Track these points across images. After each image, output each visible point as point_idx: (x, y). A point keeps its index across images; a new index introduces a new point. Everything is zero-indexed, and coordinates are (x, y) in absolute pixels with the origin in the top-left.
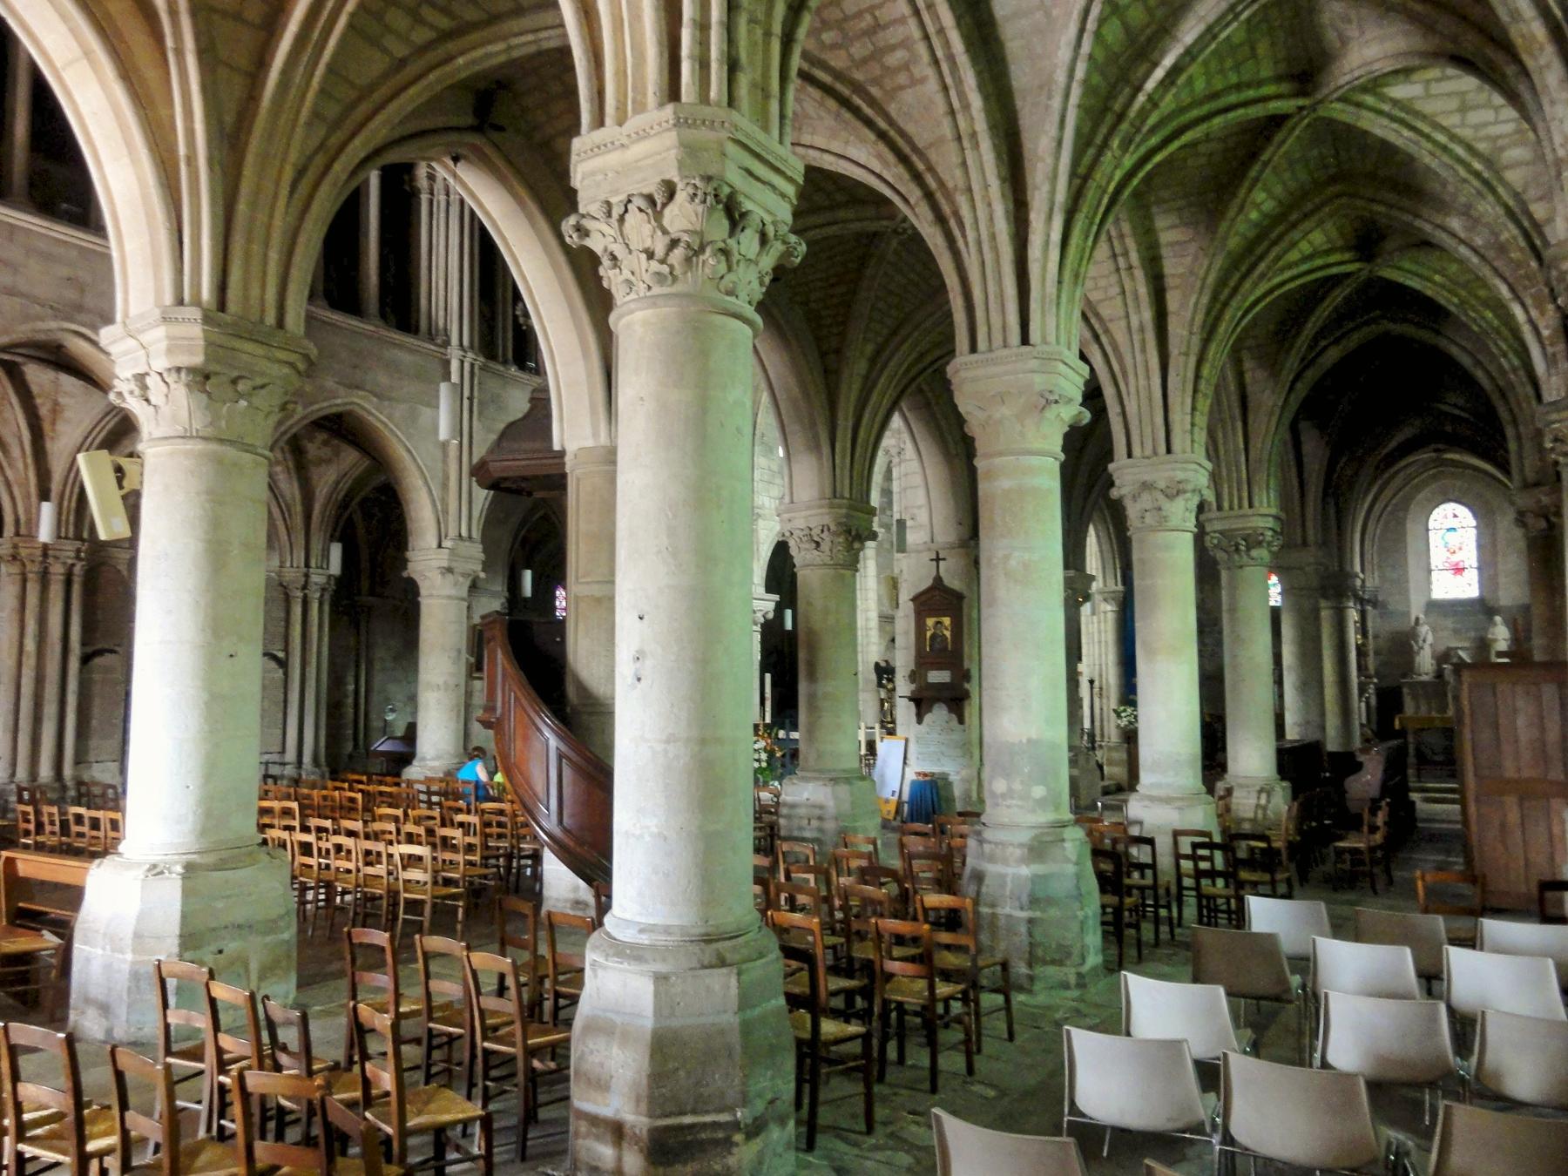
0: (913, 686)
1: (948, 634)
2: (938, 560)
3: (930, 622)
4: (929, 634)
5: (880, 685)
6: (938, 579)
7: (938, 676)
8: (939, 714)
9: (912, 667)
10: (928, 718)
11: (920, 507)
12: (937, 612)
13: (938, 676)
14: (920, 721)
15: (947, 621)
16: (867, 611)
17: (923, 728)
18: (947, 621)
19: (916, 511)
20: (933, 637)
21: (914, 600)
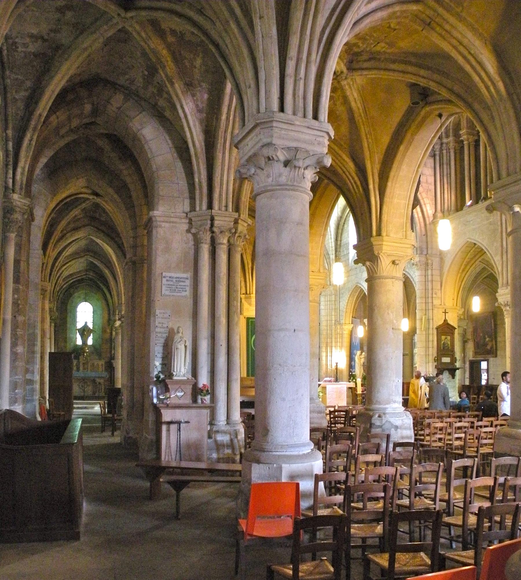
0: (436, 364)
1: (449, 343)
2: (445, 313)
3: (443, 337)
4: (442, 342)
6: (445, 320)
7: (446, 360)
9: (435, 355)
11: (438, 290)
12: (445, 334)
13: (446, 360)
15: (449, 338)
18: (449, 338)
19: (437, 291)
20: (444, 344)
21: (437, 329)
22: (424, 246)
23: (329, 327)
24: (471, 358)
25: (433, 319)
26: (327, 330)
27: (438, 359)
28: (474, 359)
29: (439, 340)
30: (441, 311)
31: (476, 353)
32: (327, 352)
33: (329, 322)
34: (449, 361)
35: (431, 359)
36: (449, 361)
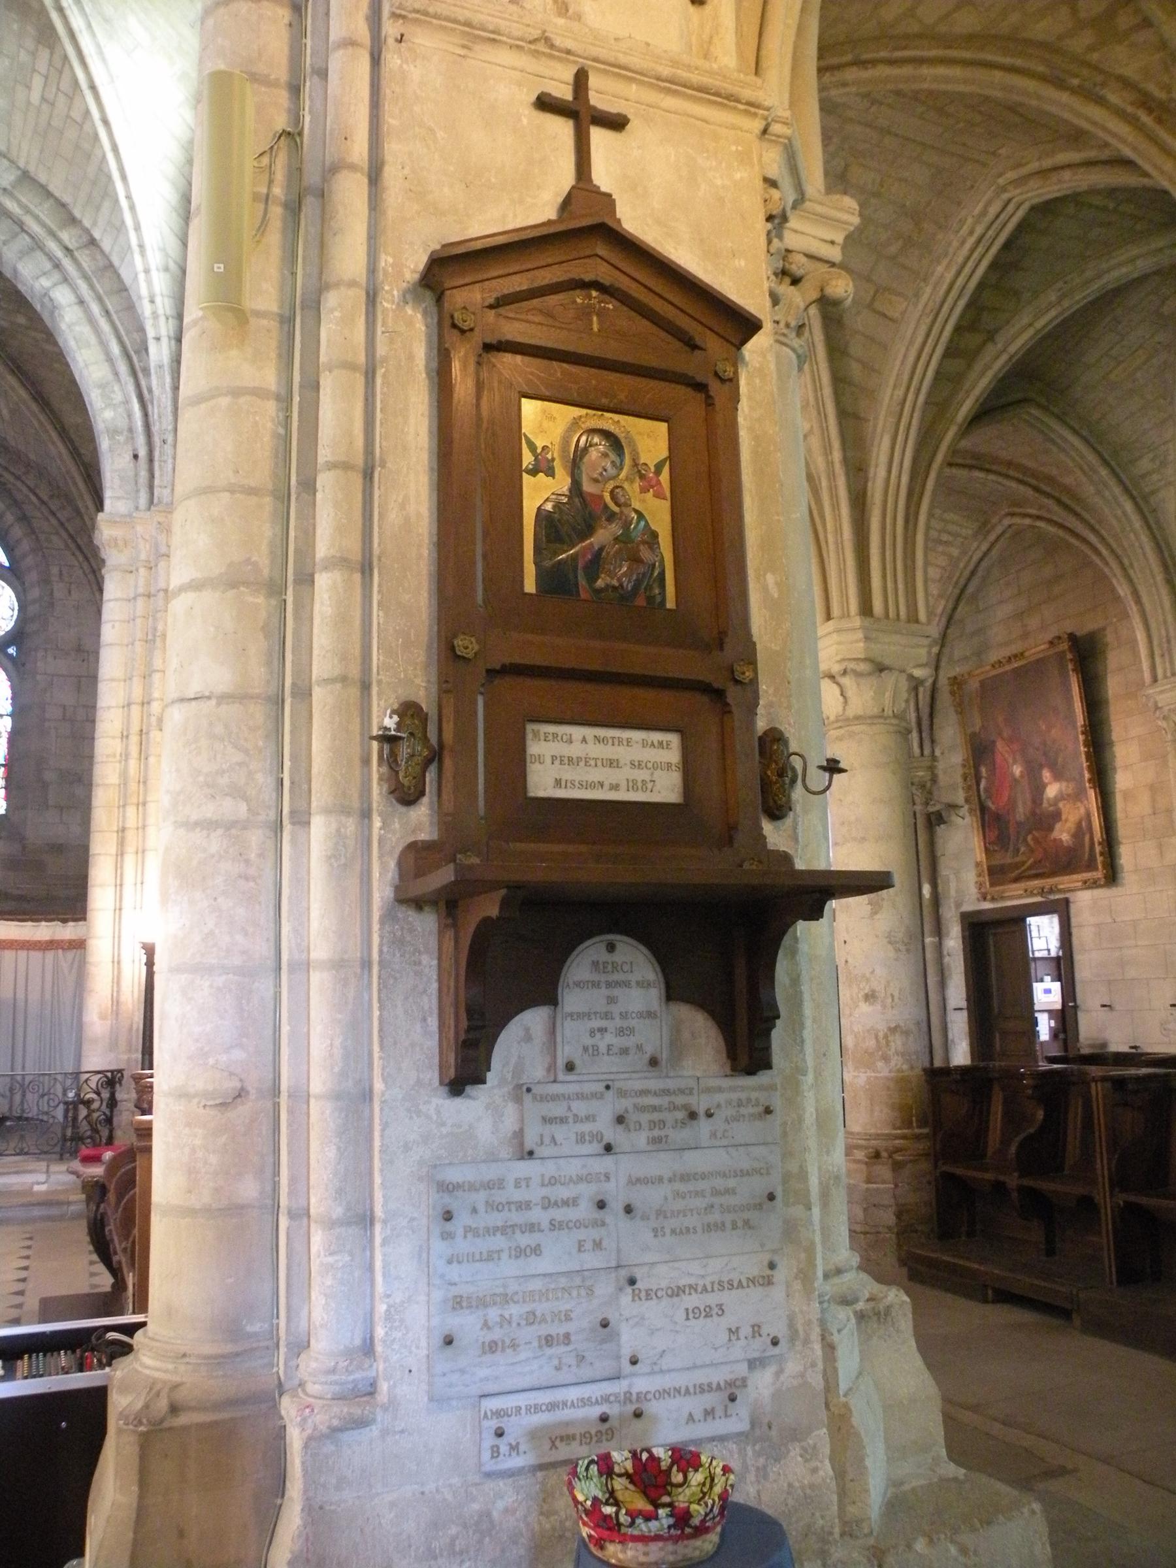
0: (421, 820)
1: (658, 514)
4: (539, 494)
8: (614, 996)
9: (406, 672)
10: (521, 1041)
14: (465, 1071)
15: (651, 441)
17: (482, 1113)
18: (651, 441)
20: (567, 523)
23: (134, 739)
24: (972, 904)
25: (375, 176)
26: (126, 756)
28: (987, 905)
29: (474, 467)
30: (511, 80)
31: (997, 874)
32: (120, 886)
33: (136, 710)
34: (666, 788)
35: (328, 743)
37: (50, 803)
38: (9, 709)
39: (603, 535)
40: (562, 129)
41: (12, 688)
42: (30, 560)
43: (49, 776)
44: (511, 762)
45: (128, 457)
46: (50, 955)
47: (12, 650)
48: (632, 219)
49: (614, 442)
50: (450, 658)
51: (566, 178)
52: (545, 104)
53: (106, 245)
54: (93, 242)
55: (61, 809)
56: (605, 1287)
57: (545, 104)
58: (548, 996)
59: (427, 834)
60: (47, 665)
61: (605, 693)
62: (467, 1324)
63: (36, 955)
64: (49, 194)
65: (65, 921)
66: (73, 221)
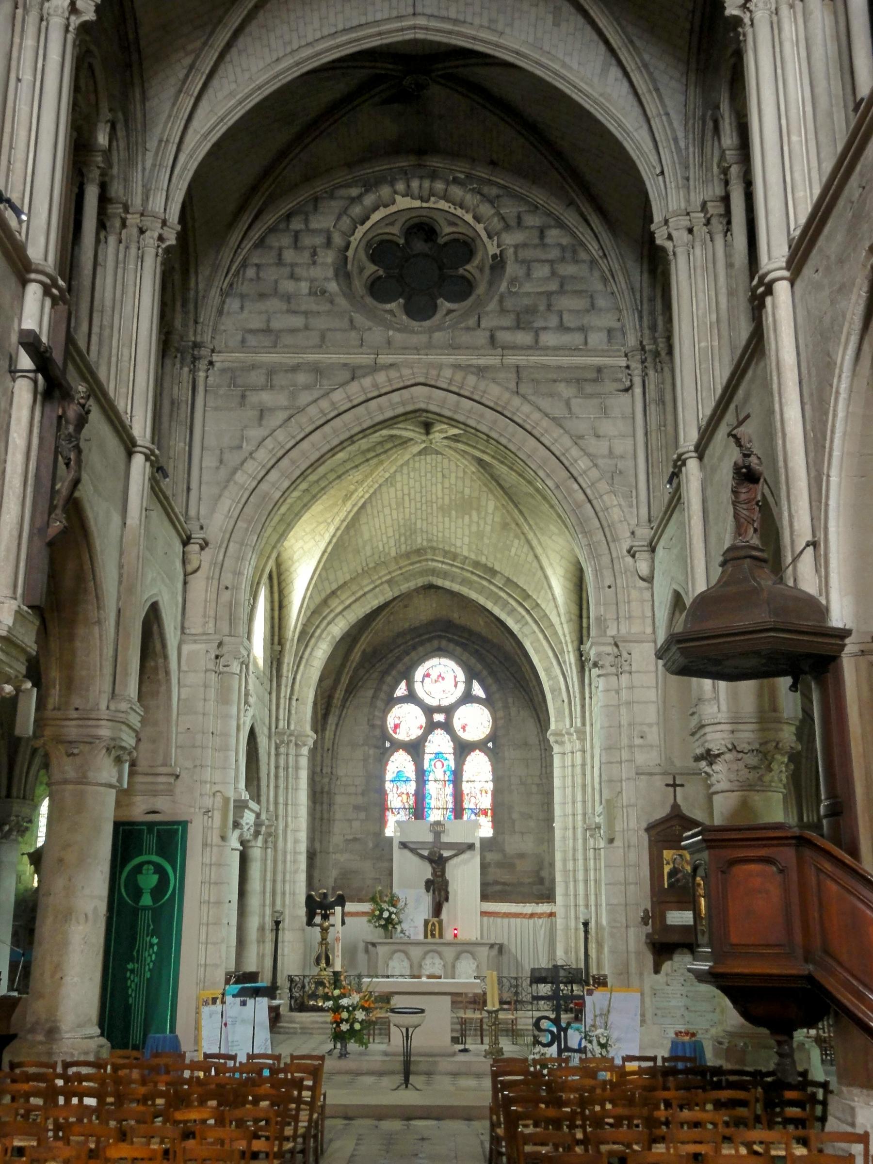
0: (649, 929)
2: (674, 785)
3: (668, 854)
4: (667, 869)
5: (310, 923)
6: (675, 806)
10: (667, 966)
11: (650, 725)
13: (679, 918)
14: (657, 971)
16: (295, 831)
17: (661, 978)
22: (611, 615)
27: (654, 916)
29: (656, 863)
34: (691, 922)
36: (691, 922)
37: (517, 828)
38: (491, 778)
39: (679, 875)
40: (671, 789)
41: (492, 765)
42: (497, 696)
43: (515, 816)
44: (663, 918)
45: (560, 702)
46: (531, 921)
47: (490, 745)
48: (686, 810)
49: (681, 856)
50: (653, 903)
51: (672, 801)
52: (667, 785)
53: (543, 606)
54: (538, 605)
55: (522, 833)
56: (683, 1009)
57: (667, 785)
58: (671, 959)
59: (650, 931)
60: (510, 753)
61: (681, 906)
62: (659, 1012)
63: (525, 921)
64: (518, 586)
65: (537, 903)
66: (528, 597)
